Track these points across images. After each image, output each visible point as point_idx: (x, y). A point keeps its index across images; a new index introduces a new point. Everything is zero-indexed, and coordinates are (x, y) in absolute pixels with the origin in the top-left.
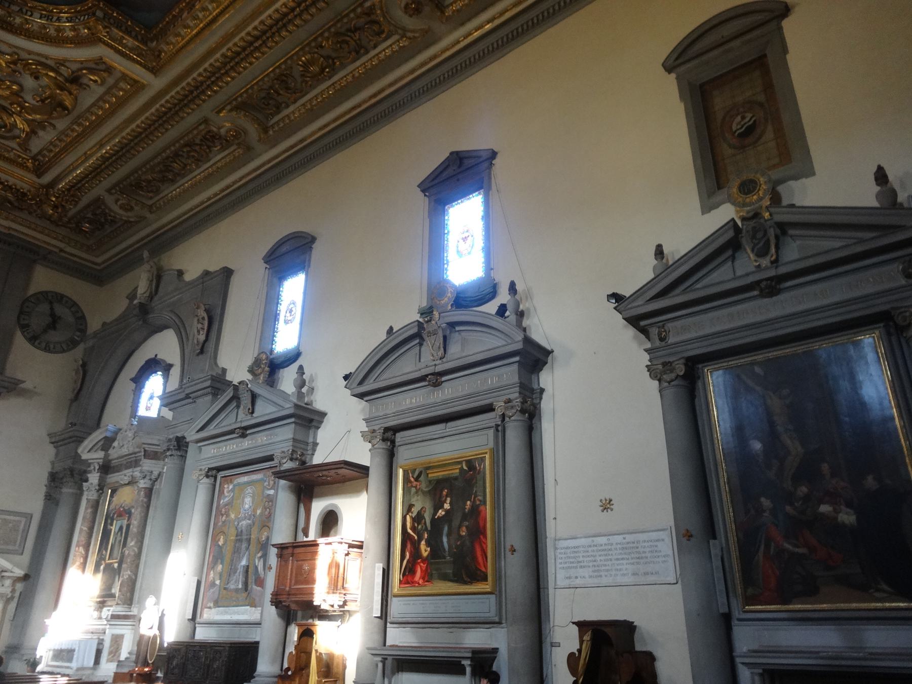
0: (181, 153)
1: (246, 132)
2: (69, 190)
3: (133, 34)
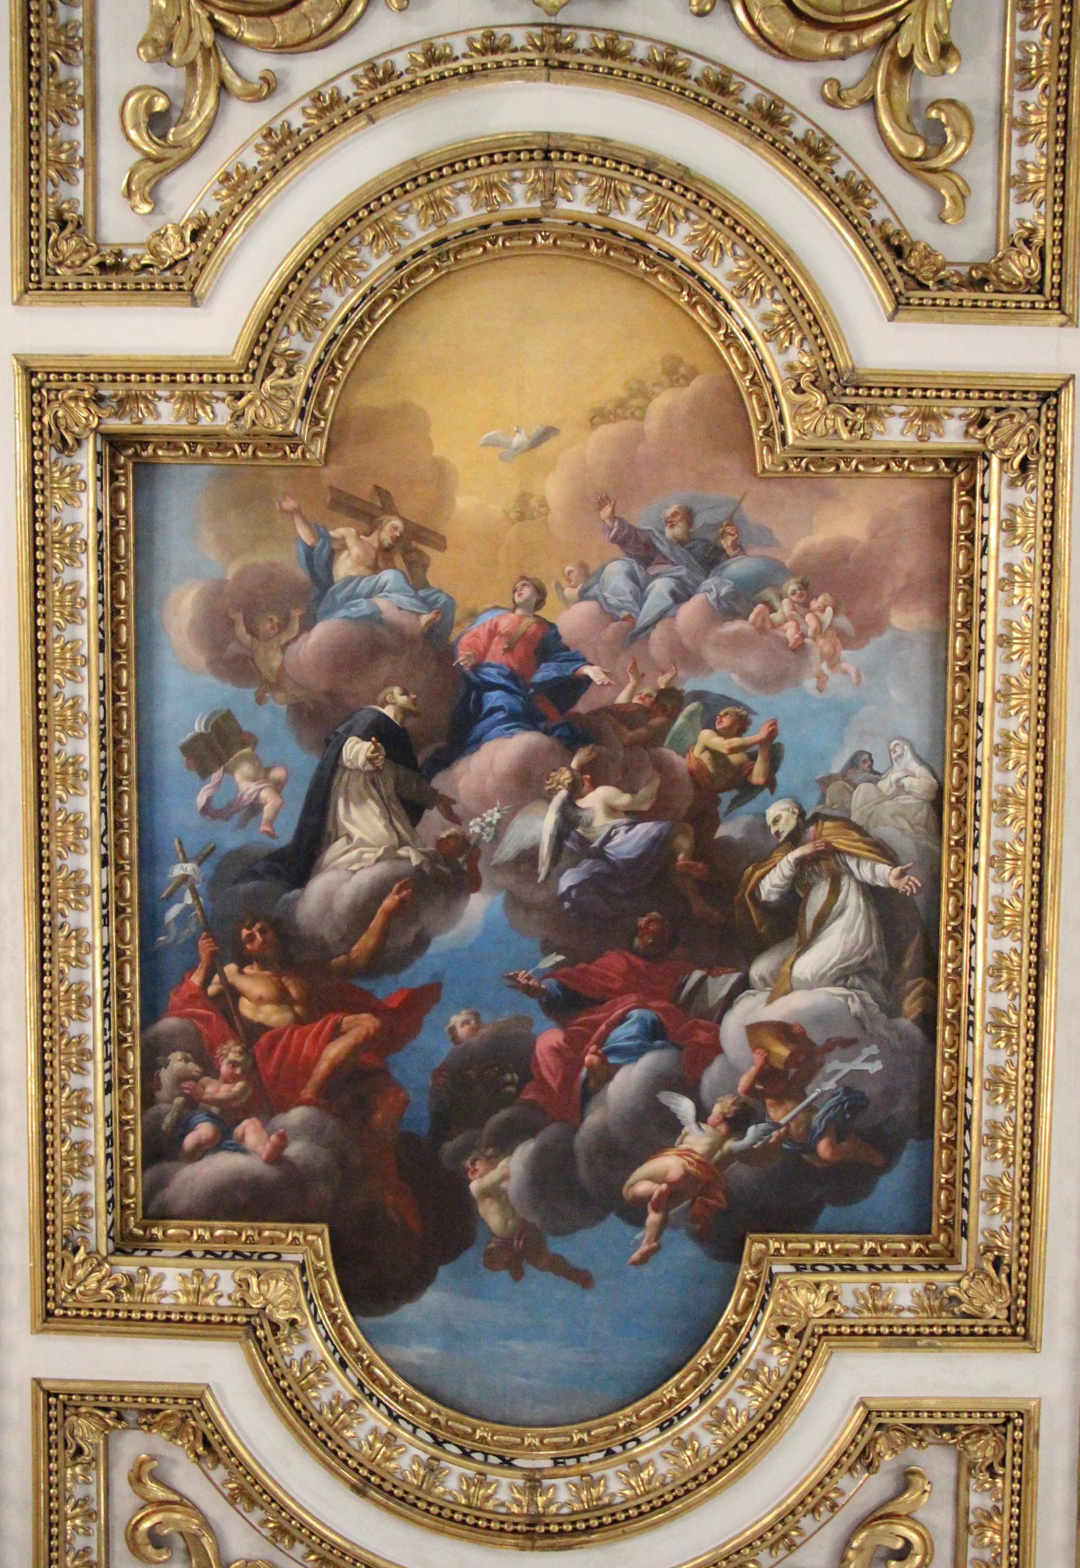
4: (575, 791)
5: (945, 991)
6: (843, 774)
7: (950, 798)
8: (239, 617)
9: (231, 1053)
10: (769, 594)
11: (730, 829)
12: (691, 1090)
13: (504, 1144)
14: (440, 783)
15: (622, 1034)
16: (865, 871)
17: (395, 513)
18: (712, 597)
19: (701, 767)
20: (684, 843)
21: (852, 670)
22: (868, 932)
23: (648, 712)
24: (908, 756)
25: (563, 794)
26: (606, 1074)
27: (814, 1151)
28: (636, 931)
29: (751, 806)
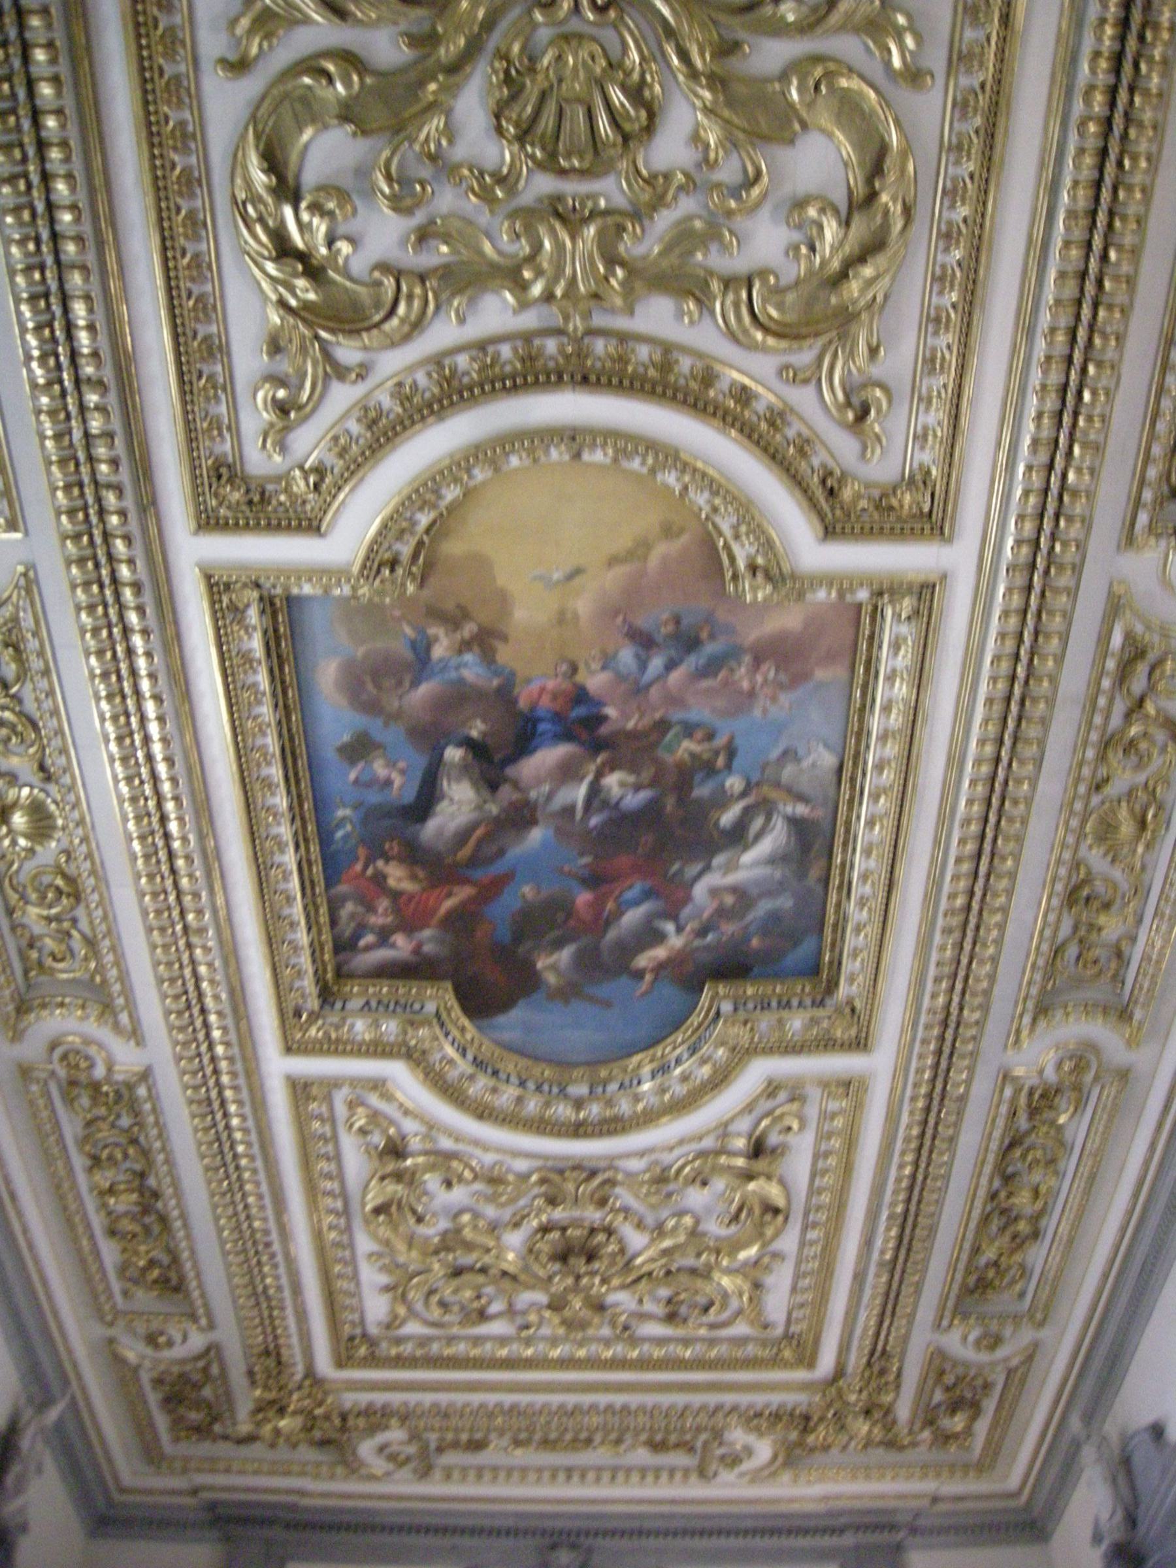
0: (1010, 1170)
2: (869, 1364)
4: (599, 775)
7: (846, 776)
8: (368, 679)
9: (383, 904)
11: (702, 791)
12: (674, 917)
13: (558, 944)
14: (510, 771)
15: (629, 895)
16: (789, 809)
20: (670, 803)
21: (787, 705)
22: (789, 836)
23: (645, 734)
24: (821, 748)
25: (589, 778)
26: (619, 913)
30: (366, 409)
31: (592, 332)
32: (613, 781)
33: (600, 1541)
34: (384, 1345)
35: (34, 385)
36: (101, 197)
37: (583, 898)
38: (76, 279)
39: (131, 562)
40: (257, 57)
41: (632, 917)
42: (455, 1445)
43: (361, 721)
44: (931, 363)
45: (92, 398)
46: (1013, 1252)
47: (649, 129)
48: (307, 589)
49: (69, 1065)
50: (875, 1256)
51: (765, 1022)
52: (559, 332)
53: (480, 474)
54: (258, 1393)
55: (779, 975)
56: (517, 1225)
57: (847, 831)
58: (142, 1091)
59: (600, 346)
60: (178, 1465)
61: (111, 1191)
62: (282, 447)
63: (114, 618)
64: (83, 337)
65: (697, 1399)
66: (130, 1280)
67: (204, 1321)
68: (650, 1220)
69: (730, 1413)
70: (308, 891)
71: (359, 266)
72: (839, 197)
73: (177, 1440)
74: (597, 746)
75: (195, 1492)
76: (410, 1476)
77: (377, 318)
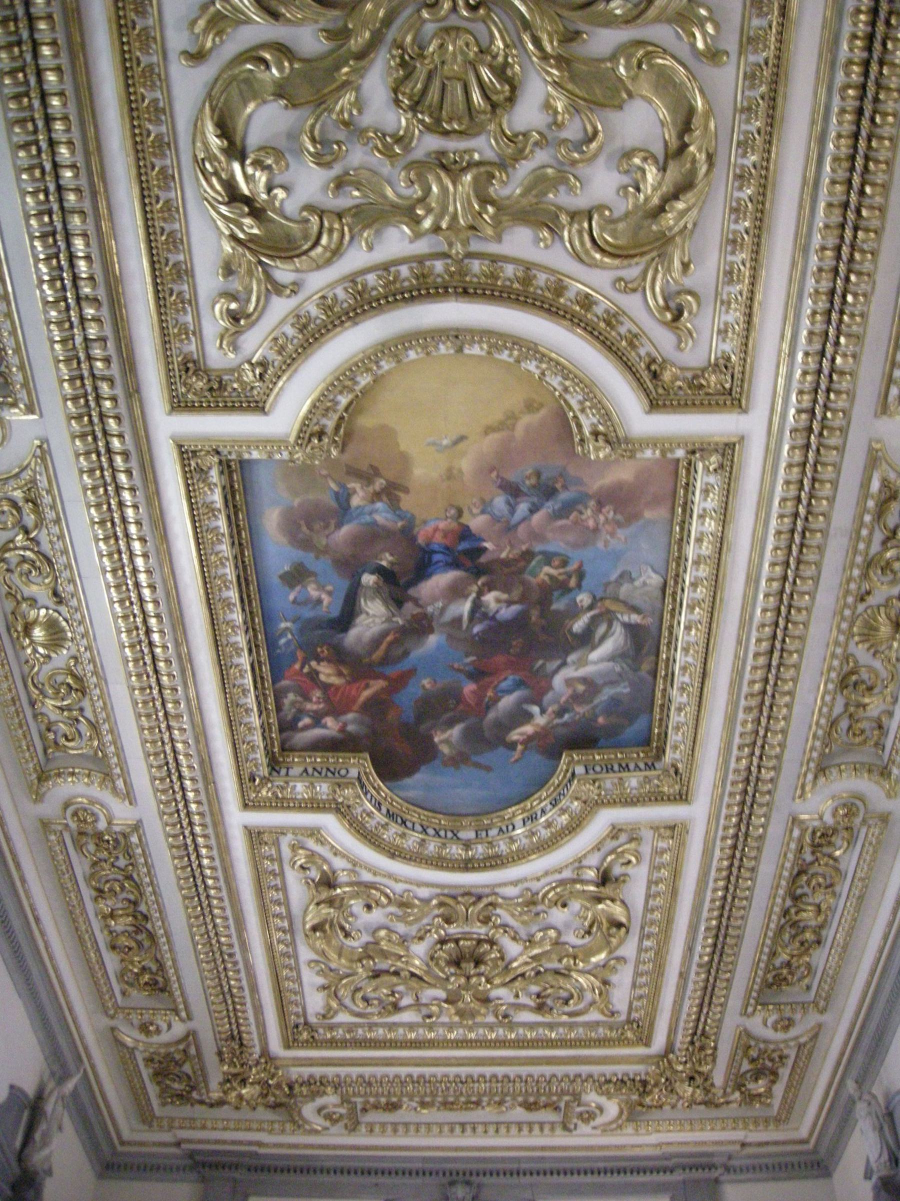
0: (799, 891)
1: (861, 798)
2: (692, 1043)
3: (632, 766)
4: (480, 593)
5: (662, 665)
6: (616, 581)
7: (669, 591)
8: (302, 523)
9: (317, 694)
10: (580, 507)
11: (559, 605)
12: (538, 702)
13: (451, 724)
14: (412, 592)
15: (504, 685)
16: (626, 618)
17: (382, 477)
18: (550, 511)
19: (544, 581)
20: (534, 614)
21: (623, 538)
22: (626, 641)
23: (516, 561)
24: (650, 570)
25: (474, 595)
26: (496, 700)
27: (596, 721)
28: (511, 647)
29: (571, 595)
30: (298, 317)
31: (470, 255)
32: (490, 598)
33: (487, 1180)
34: (321, 1031)
35: (46, 303)
36: (94, 160)
37: (469, 688)
38: (76, 220)
39: (121, 436)
40: (211, 49)
41: (507, 702)
42: (376, 1107)
43: (298, 555)
44: (730, 275)
45: (90, 312)
46: (800, 956)
47: (511, 99)
48: (255, 455)
49: (79, 820)
50: (696, 958)
51: (609, 781)
52: (445, 255)
53: (386, 365)
54: (226, 1068)
55: (619, 746)
56: (421, 938)
57: (671, 633)
58: (134, 839)
59: (476, 266)
60: (165, 1123)
61: (112, 916)
62: (235, 347)
63: (109, 479)
64: (82, 265)
65: (560, 1070)
66: (127, 983)
67: (183, 1014)
68: (523, 934)
69: (586, 1080)
70: (259, 686)
71: (292, 207)
72: (658, 149)
73: (164, 1104)
74: (478, 572)
75: (178, 1144)
76: (344, 1131)
77: (306, 247)
